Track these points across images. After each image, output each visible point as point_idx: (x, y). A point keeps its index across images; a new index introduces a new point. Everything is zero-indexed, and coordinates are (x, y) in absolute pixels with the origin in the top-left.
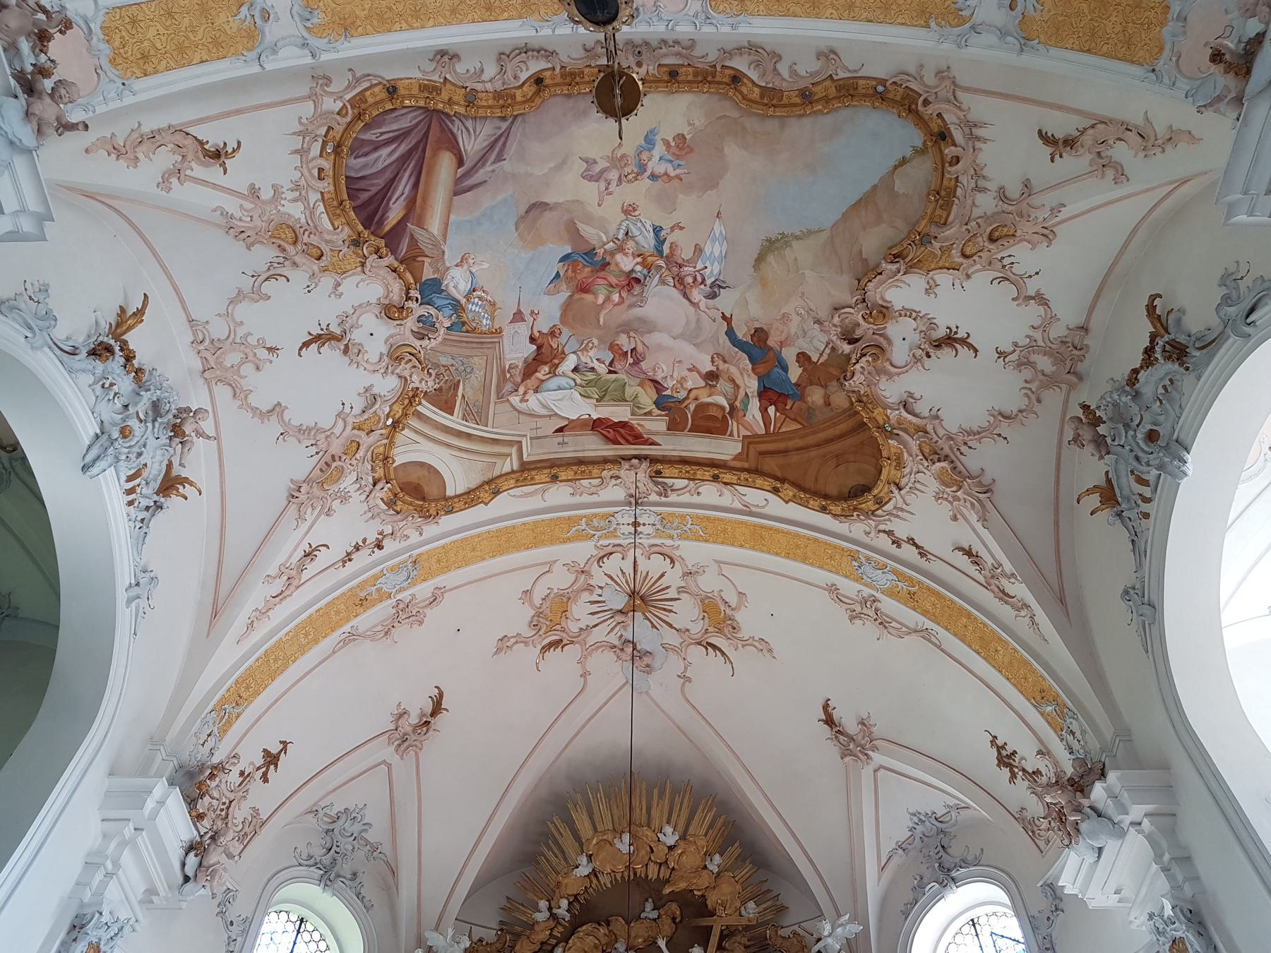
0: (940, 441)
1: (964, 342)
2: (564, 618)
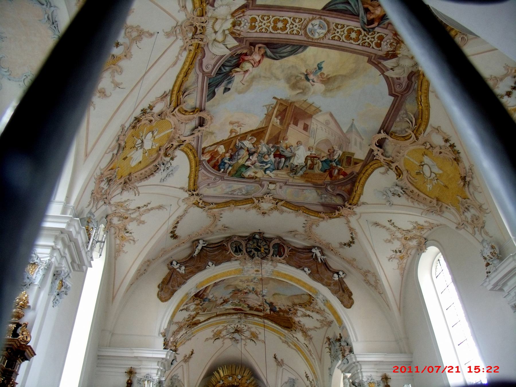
1: (311, 317)
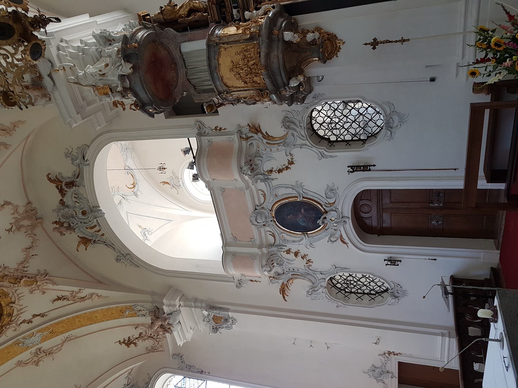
0: (14, 274)
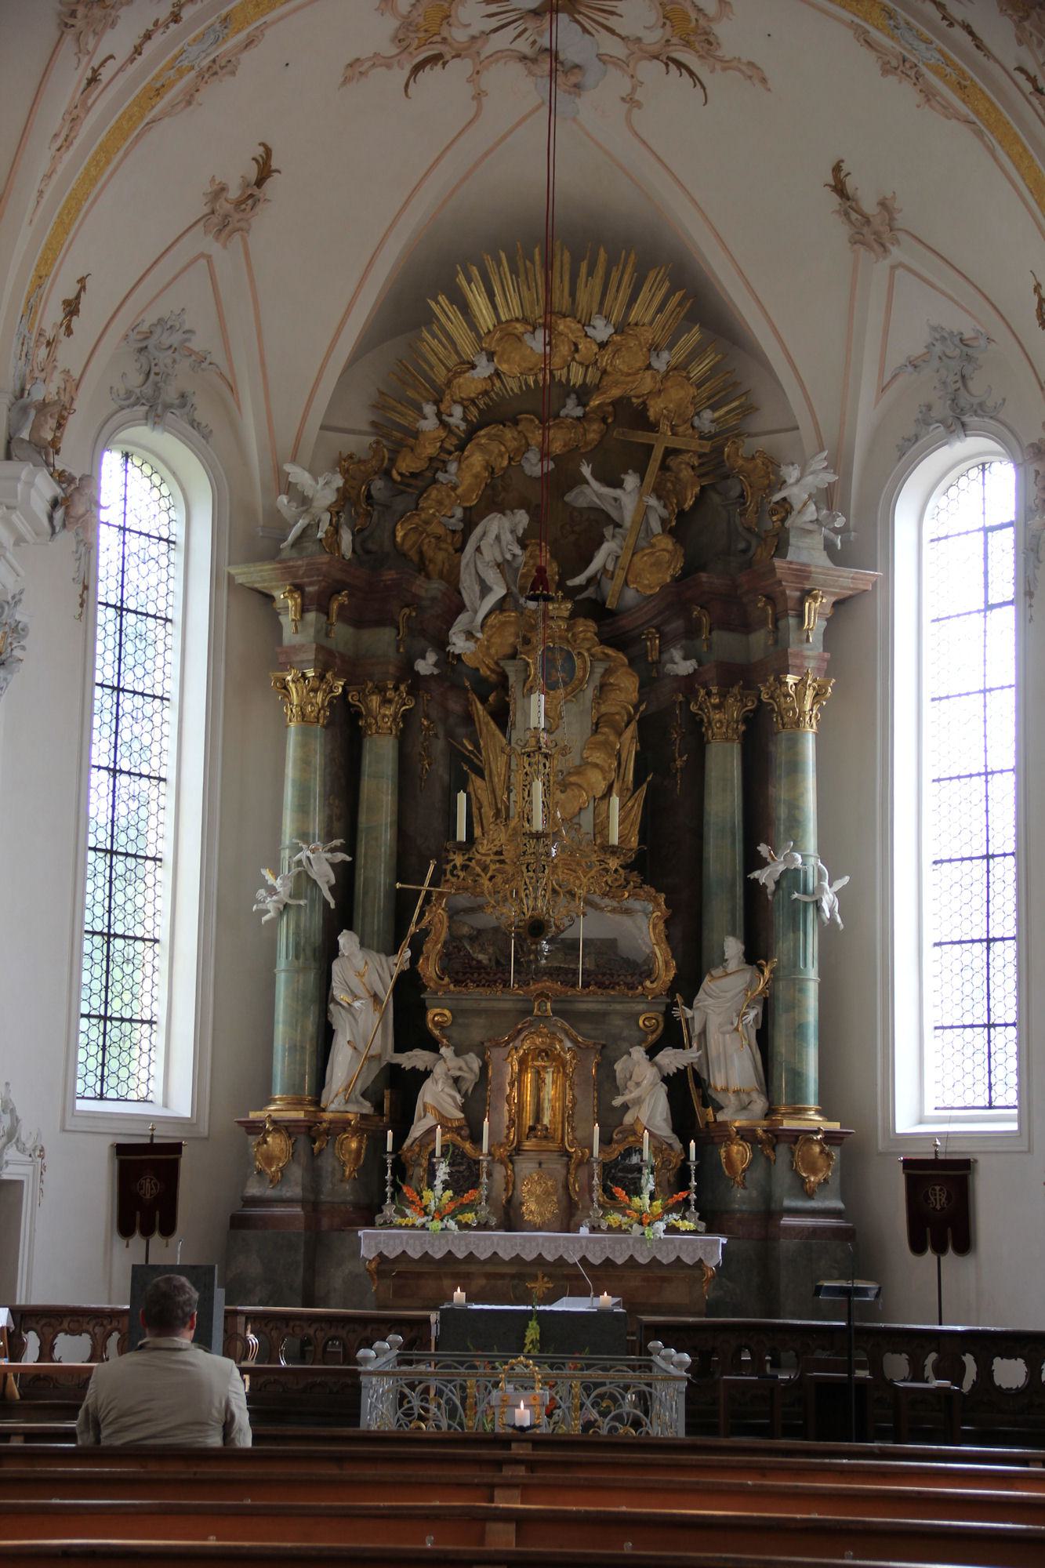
2: (445, 25)
